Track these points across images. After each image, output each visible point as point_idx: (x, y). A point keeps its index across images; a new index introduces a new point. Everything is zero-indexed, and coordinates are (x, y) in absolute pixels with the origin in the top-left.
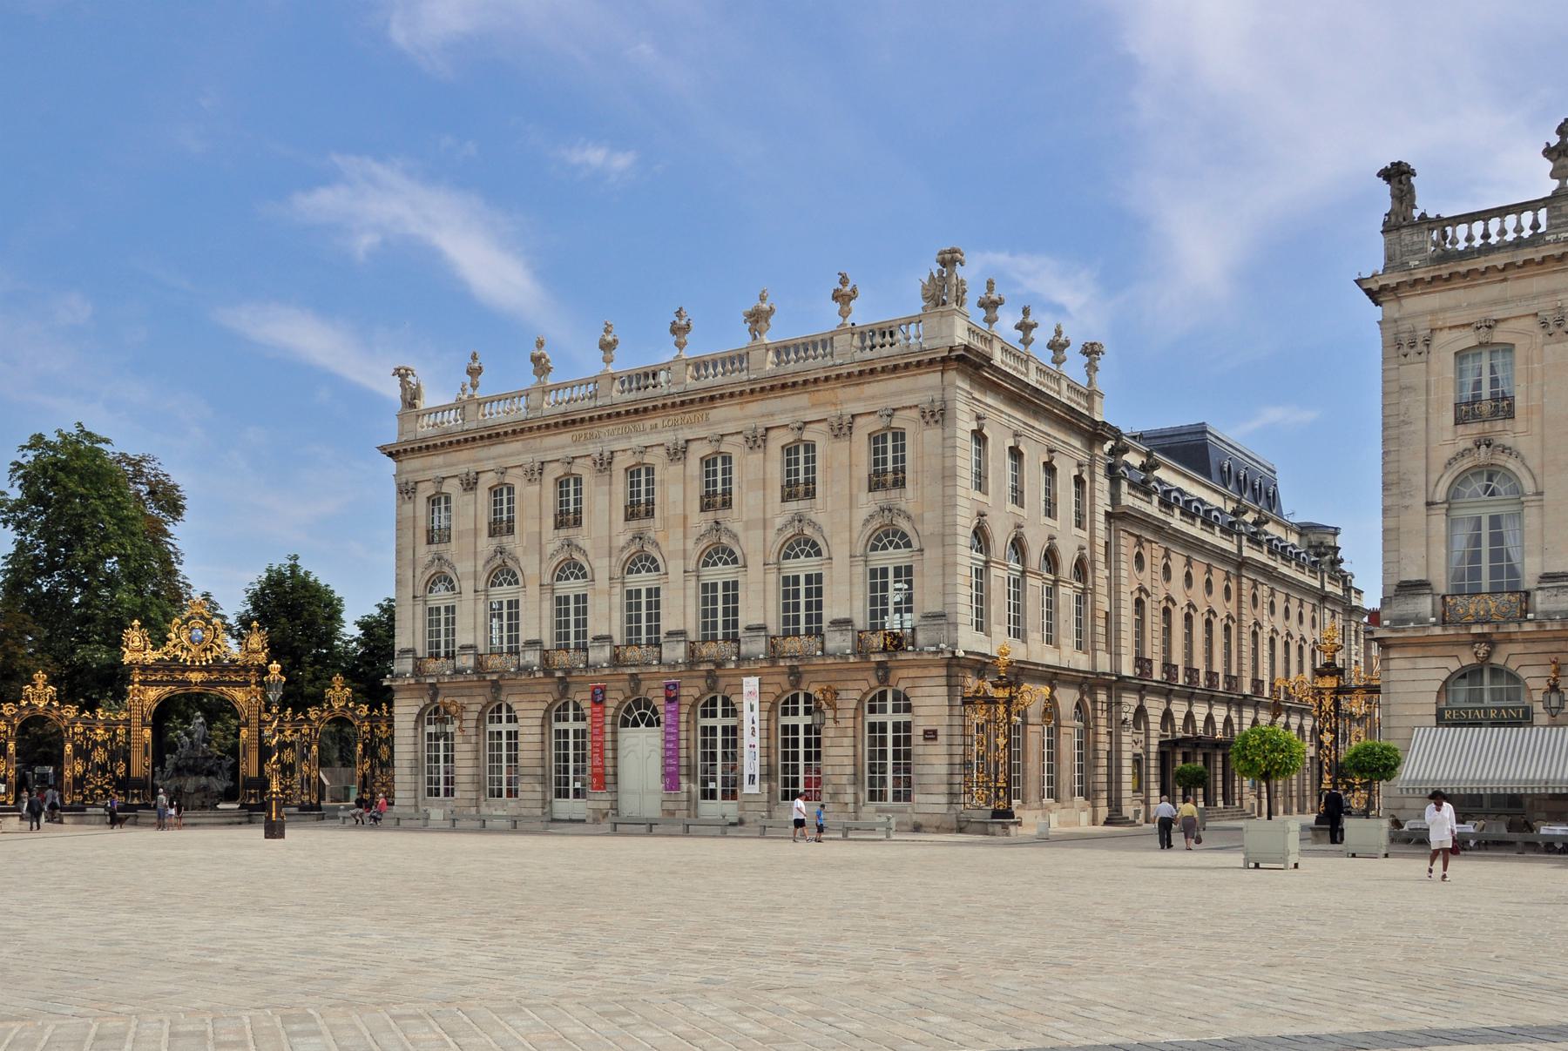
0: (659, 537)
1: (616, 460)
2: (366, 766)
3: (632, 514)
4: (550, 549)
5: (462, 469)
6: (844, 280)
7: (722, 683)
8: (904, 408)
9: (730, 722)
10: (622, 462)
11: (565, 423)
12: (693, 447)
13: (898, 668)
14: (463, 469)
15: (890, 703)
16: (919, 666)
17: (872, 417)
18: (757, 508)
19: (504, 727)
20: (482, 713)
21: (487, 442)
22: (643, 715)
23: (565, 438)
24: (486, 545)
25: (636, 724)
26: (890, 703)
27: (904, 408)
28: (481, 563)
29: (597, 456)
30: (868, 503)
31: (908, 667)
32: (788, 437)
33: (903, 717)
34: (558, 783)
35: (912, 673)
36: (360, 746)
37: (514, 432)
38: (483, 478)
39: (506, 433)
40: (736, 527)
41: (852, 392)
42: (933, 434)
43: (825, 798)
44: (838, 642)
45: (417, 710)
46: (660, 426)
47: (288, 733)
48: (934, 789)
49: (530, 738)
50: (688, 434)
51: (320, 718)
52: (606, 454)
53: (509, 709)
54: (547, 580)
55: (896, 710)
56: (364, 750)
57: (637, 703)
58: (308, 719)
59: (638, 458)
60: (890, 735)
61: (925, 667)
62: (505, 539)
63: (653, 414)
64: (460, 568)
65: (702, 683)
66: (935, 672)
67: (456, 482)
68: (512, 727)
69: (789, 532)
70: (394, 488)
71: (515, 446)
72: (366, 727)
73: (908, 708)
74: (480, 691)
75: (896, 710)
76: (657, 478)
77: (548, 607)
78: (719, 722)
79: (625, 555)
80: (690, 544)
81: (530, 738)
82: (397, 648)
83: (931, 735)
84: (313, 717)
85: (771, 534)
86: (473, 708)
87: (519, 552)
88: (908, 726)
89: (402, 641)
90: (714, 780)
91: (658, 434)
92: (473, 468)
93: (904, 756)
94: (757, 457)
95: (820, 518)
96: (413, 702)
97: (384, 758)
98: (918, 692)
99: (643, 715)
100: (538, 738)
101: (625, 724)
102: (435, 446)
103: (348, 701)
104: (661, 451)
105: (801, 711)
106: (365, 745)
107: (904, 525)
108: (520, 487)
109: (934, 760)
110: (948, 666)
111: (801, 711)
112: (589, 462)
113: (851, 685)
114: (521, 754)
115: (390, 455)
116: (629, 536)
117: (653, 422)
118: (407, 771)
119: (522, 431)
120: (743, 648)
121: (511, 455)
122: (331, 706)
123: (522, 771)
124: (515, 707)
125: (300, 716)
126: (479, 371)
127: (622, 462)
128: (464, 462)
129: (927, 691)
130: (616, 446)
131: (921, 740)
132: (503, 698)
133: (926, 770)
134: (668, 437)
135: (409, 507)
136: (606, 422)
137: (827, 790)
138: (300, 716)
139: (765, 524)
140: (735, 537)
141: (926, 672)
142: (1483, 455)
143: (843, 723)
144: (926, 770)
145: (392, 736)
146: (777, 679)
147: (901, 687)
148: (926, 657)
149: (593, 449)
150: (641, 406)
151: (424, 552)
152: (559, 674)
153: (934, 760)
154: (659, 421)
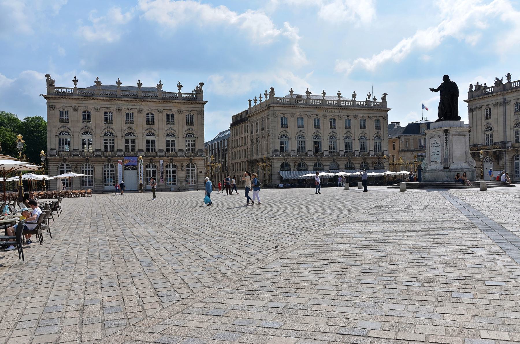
0: (135, 128)
3: (127, 122)
4: (103, 128)
6: (180, 83)
7: (154, 161)
14: (73, 105)
18: (160, 124)
24: (81, 125)
28: (79, 130)
30: (186, 127)
38: (80, 108)
40: (155, 129)
41: (183, 105)
42: (199, 116)
45: (58, 165)
50: (143, 107)
54: (102, 135)
60: (191, 172)
62: (88, 124)
64: (72, 129)
65: (149, 161)
69: (168, 131)
76: (134, 115)
77: (102, 142)
79: (126, 132)
80: (144, 131)
83: (201, 172)
85: (164, 131)
87: (93, 128)
94: (160, 115)
95: (175, 129)
100: (101, 172)
108: (93, 113)
116: (127, 127)
126: (77, 81)
127: (125, 111)
128: (75, 103)
134: (138, 107)
135: (52, 112)
139: (163, 129)
140: (155, 130)
142: (285, 133)
151: (59, 124)
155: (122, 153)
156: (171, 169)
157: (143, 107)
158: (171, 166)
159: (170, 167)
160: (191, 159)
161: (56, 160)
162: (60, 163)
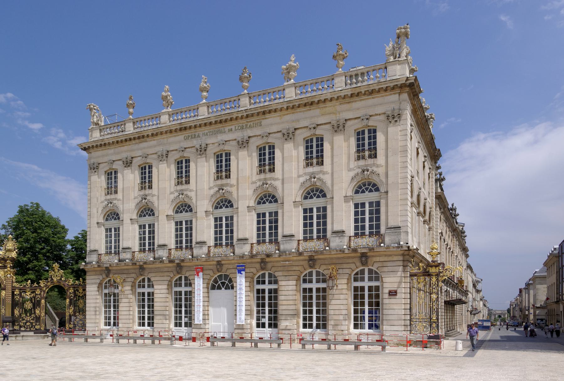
1: (208, 149)
2: (71, 311)
5: (124, 155)
7: (269, 265)
8: (376, 115)
9: (273, 287)
10: (212, 150)
11: (181, 129)
12: (252, 140)
13: (373, 256)
15: (366, 276)
16: (386, 255)
17: (356, 121)
19: (146, 290)
20: (134, 283)
21: (137, 141)
22: (223, 284)
23: (180, 137)
25: (219, 288)
26: (366, 276)
27: (376, 115)
29: (198, 146)
31: (380, 256)
32: (307, 134)
33: (374, 284)
34: (176, 318)
35: (382, 259)
36: (68, 300)
37: (152, 135)
39: (148, 136)
43: (330, 327)
44: (335, 242)
45: (98, 281)
46: (233, 129)
47: (28, 294)
48: (396, 323)
49: (161, 296)
50: (250, 133)
51: (46, 286)
52: (203, 146)
53: (149, 280)
55: (370, 279)
56: (70, 302)
57: (220, 277)
58: (40, 286)
59: (222, 147)
60: (366, 293)
61: (390, 256)
63: (231, 123)
65: (258, 266)
66: (395, 258)
67: (121, 162)
68: (150, 290)
70: (87, 167)
71: (152, 142)
72: (71, 291)
73: (377, 279)
74: (133, 271)
75: (370, 279)
78: (267, 287)
81: (161, 296)
82: (88, 249)
83: (393, 293)
84: (42, 285)
86: (129, 280)
88: (377, 288)
89: (91, 246)
90: (264, 317)
91: (231, 135)
92: (130, 155)
93: (376, 305)
96: (96, 277)
97: (81, 306)
98: (386, 269)
99: (223, 284)
101: (213, 288)
102: (109, 144)
103: (62, 277)
104: (234, 143)
105: (314, 281)
106: (71, 300)
107: (375, 179)
109: (395, 307)
110: (403, 255)
111: (314, 281)
112: (194, 150)
113: (345, 266)
114: (155, 304)
115: (85, 149)
117: (230, 128)
118: (93, 313)
119: (157, 134)
120: (282, 247)
121: (150, 147)
122: (52, 279)
123: (155, 313)
124: (152, 279)
125: (35, 285)
127: (212, 150)
129: (391, 269)
130: (209, 141)
131: (386, 296)
132: (146, 274)
133: (390, 312)
134: (239, 135)
136: (203, 128)
137: (331, 323)
138: (35, 285)
141: (390, 258)
143: (340, 287)
144: (390, 312)
145: (85, 295)
146: (301, 263)
147: (374, 268)
148: (392, 249)
149: (196, 143)
150: (224, 118)
152: (177, 261)
153: (395, 307)
154: (233, 127)
155: (205, 250)
156: (314, 286)
157: (250, 133)
158: (314, 278)
159: (311, 281)
160: (364, 255)
161: (94, 271)
162: (101, 277)
